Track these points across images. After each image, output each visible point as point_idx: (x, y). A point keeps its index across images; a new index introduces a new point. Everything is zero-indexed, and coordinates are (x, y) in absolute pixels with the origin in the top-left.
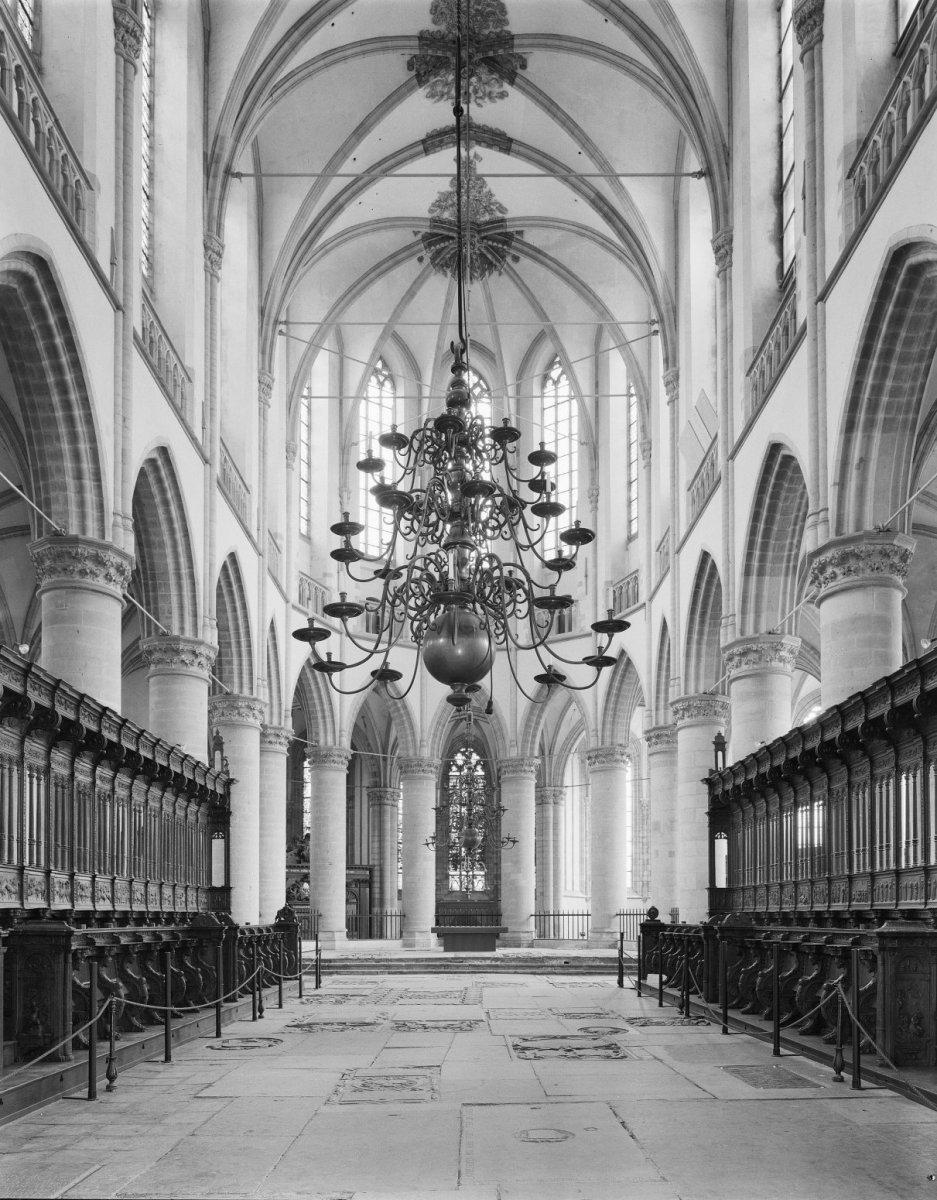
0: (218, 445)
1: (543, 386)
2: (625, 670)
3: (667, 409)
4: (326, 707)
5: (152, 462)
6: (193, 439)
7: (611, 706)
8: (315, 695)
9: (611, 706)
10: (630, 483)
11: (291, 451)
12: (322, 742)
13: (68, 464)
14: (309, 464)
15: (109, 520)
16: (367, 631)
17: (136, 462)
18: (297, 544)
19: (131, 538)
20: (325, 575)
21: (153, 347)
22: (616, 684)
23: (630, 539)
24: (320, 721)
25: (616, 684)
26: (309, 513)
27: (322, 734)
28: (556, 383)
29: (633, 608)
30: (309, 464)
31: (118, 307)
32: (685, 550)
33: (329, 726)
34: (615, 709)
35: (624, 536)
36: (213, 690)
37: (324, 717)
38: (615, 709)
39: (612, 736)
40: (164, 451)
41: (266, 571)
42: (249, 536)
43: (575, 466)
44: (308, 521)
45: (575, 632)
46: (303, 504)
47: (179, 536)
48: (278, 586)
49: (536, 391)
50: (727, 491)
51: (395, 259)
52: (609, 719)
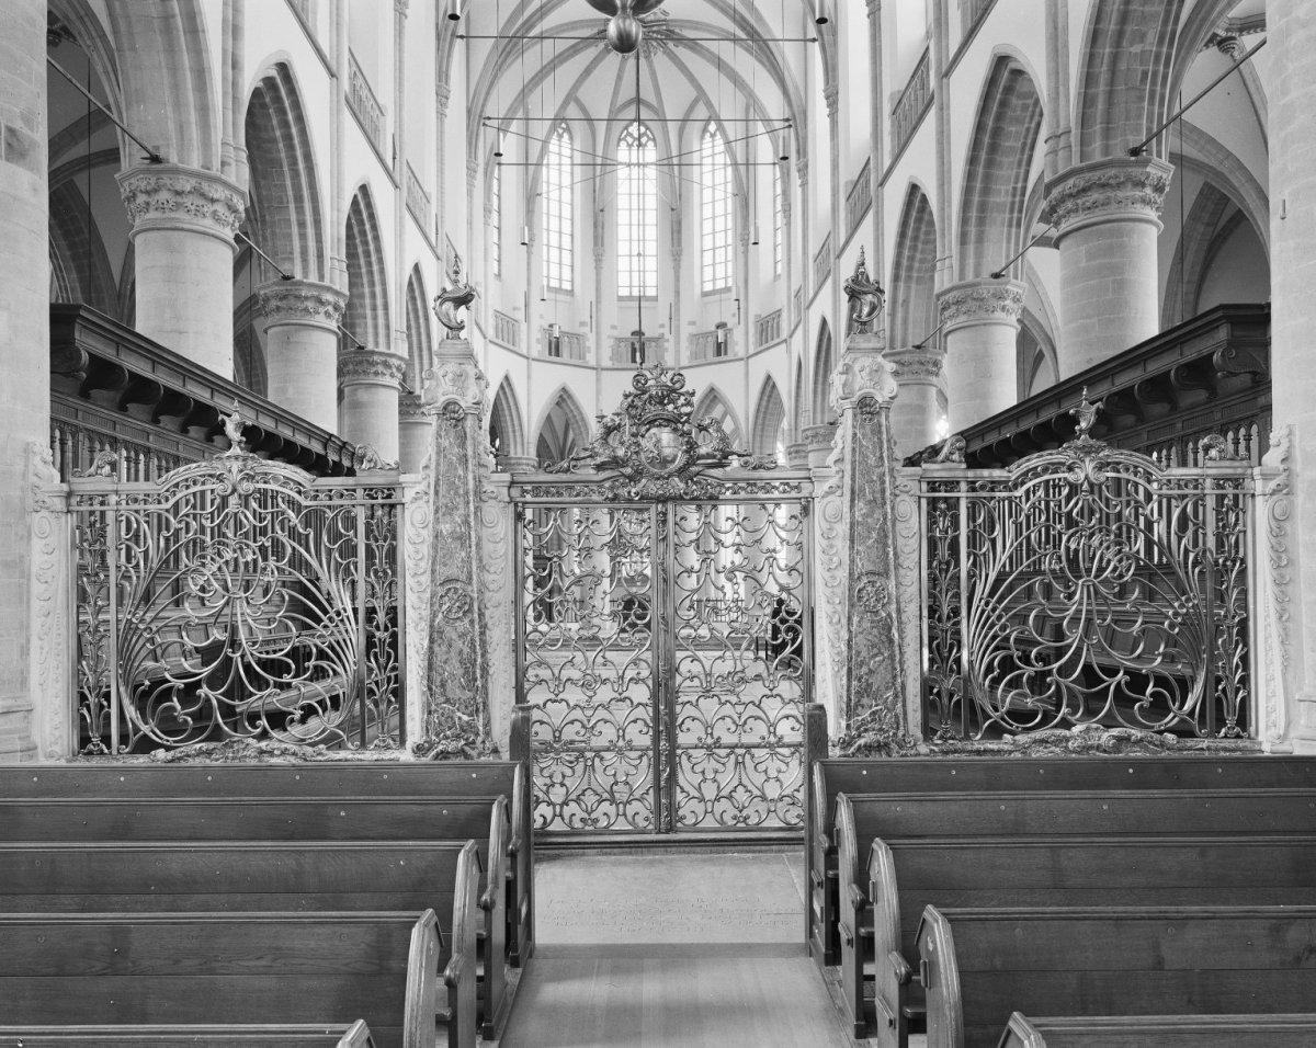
0: (346, 56)
1: (702, 138)
2: (772, 392)
3: (799, 190)
4: (516, 422)
5: (269, 81)
6: (318, 51)
7: (760, 421)
8: (507, 412)
9: (760, 421)
10: (776, 230)
11: (487, 211)
12: (512, 454)
13: (368, 301)
14: (499, 212)
15: (328, 264)
16: (550, 354)
17: (250, 81)
18: (493, 284)
19: (246, 171)
20: (514, 309)
21: (359, 105)
22: (764, 403)
23: (776, 277)
24: (511, 434)
25: (764, 403)
26: (499, 256)
27: (512, 446)
28: (713, 136)
29: (771, 343)
30: (499, 212)
31: (332, 75)
32: (812, 307)
33: (519, 440)
34: (763, 424)
35: (771, 276)
36: (343, 342)
37: (514, 431)
38: (763, 424)
39: (761, 448)
40: (283, 68)
41: (343, 102)
42: (426, 238)
43: (730, 209)
44: (499, 261)
45: (730, 356)
46: (495, 247)
47: (422, 320)
48: (480, 329)
49: (696, 147)
50: (877, 212)
51: (574, 51)
52: (759, 433)
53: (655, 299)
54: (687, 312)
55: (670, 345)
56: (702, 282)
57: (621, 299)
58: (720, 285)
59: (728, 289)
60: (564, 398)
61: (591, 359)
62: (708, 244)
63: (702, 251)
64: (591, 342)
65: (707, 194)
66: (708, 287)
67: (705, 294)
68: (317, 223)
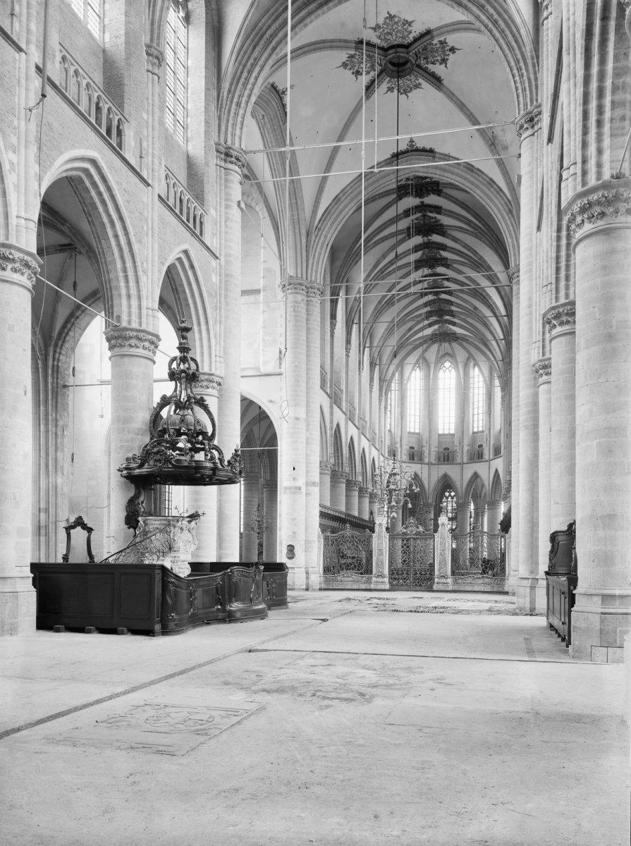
45: (483, 460)
53: (454, 434)
54: (466, 441)
55: (459, 454)
56: (473, 427)
57: (439, 435)
58: (481, 429)
59: (483, 432)
60: (416, 477)
61: (426, 460)
62: (476, 412)
63: (473, 415)
64: (426, 454)
65: (476, 391)
66: (476, 430)
67: (474, 433)
68: (342, 455)
